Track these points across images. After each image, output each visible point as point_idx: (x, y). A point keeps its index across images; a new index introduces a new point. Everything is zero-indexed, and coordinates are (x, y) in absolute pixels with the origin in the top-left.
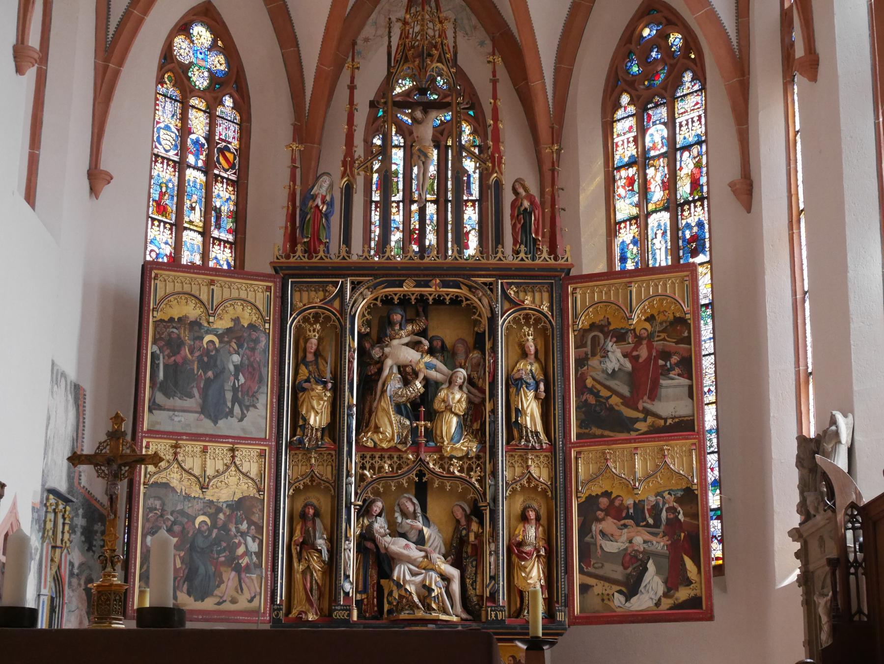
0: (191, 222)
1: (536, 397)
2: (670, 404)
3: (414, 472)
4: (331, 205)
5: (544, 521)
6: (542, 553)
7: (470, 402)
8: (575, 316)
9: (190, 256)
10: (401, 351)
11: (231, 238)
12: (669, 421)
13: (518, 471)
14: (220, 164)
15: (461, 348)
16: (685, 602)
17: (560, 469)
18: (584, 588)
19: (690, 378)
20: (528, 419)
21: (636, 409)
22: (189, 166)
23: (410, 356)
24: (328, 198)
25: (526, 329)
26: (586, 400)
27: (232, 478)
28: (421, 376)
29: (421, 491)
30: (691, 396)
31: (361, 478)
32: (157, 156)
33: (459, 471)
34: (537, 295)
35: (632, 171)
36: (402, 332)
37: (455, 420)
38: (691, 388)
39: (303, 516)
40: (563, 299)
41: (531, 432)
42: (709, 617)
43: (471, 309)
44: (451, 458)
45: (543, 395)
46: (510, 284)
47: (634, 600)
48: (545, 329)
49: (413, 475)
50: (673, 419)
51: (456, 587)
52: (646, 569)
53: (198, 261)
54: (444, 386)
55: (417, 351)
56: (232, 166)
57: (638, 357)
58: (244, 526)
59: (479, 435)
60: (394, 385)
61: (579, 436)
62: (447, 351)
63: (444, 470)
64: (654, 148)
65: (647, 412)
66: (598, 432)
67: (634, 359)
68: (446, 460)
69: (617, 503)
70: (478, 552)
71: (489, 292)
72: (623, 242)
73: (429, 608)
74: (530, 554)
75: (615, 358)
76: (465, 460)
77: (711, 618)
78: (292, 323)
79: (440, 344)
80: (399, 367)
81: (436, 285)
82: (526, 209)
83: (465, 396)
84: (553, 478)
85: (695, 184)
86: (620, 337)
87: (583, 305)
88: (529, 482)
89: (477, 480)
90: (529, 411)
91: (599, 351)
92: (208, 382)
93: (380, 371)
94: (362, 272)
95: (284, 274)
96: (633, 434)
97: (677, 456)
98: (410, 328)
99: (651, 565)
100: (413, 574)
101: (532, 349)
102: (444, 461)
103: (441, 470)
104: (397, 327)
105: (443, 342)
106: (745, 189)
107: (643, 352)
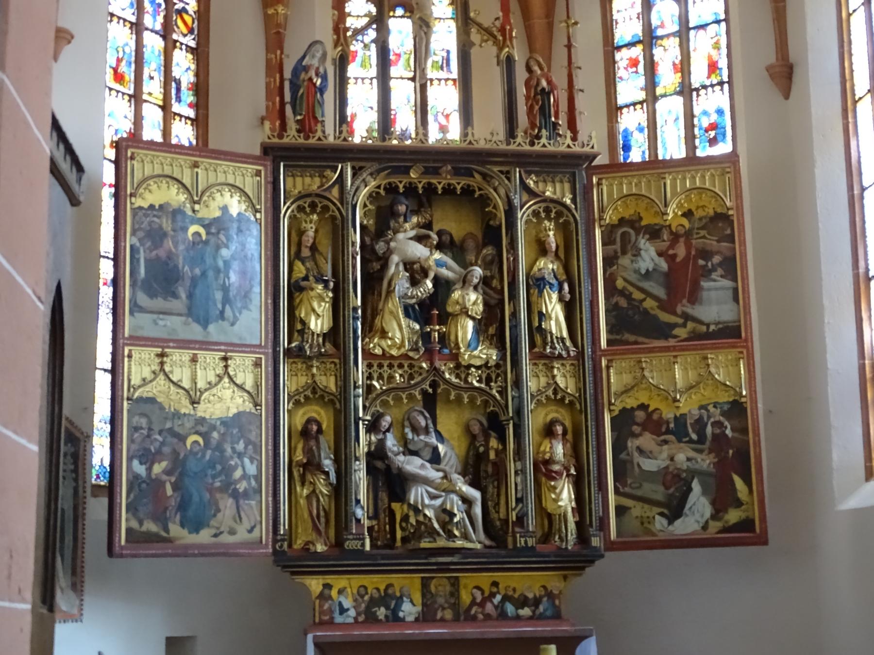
0: (150, 94)
1: (561, 299)
2: (714, 306)
3: (428, 383)
4: (324, 78)
5: (569, 437)
6: (573, 471)
7: (486, 304)
8: (602, 210)
9: (152, 132)
10: (406, 244)
11: (191, 113)
12: (712, 327)
13: (543, 380)
14: (178, 27)
15: (470, 244)
16: (735, 525)
17: (589, 379)
18: (621, 510)
19: (735, 280)
20: (553, 323)
21: (674, 313)
22: (147, 29)
23: (419, 251)
24: (321, 70)
25: (547, 223)
26: (617, 303)
27: (226, 391)
28: (432, 275)
29: (430, 402)
30: (736, 299)
31: (369, 389)
32: (112, 15)
33: (478, 381)
34: (558, 185)
35: (637, 51)
36: (407, 225)
37: (470, 324)
38: (735, 290)
39: (305, 433)
40: (588, 190)
41: (557, 338)
42: (762, 540)
43: (485, 200)
44: (469, 366)
45: (568, 297)
46: (529, 173)
47: (678, 523)
48: (567, 223)
49: (426, 386)
50: (717, 324)
51: (478, 510)
52: (690, 489)
53: (159, 139)
54: (457, 286)
55: (425, 246)
56: (191, 31)
57: (674, 256)
58: (241, 446)
59: (499, 341)
60: (402, 285)
61: (609, 342)
62: (456, 246)
63: (460, 379)
64: (662, 26)
65: (687, 317)
66: (632, 338)
67: (671, 259)
68: (463, 369)
69: (655, 417)
70: (500, 473)
71: (506, 182)
72: (626, 130)
73: (451, 536)
74: (559, 474)
75: (649, 256)
76: (484, 369)
77: (765, 543)
78: (286, 211)
79: (449, 238)
80: (405, 264)
81: (448, 172)
82: (543, 89)
83: (481, 297)
84: (582, 390)
85: (713, 67)
86: (654, 233)
87: (610, 198)
88: (555, 392)
89: (497, 392)
90: (553, 316)
91: (628, 247)
92: (194, 281)
93: (385, 266)
94: (361, 156)
95: (274, 155)
96: (672, 342)
97: (724, 367)
98: (415, 220)
99: (696, 486)
100: (433, 497)
101: (554, 246)
102: (461, 369)
103: (457, 381)
104: (401, 219)
105: (451, 235)
106: (784, 74)
107: (681, 251)
